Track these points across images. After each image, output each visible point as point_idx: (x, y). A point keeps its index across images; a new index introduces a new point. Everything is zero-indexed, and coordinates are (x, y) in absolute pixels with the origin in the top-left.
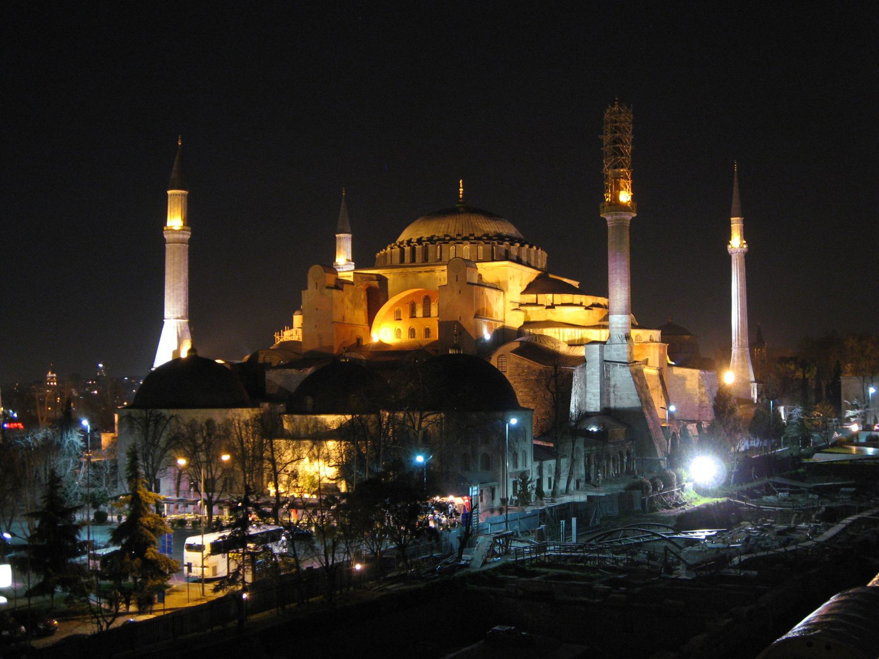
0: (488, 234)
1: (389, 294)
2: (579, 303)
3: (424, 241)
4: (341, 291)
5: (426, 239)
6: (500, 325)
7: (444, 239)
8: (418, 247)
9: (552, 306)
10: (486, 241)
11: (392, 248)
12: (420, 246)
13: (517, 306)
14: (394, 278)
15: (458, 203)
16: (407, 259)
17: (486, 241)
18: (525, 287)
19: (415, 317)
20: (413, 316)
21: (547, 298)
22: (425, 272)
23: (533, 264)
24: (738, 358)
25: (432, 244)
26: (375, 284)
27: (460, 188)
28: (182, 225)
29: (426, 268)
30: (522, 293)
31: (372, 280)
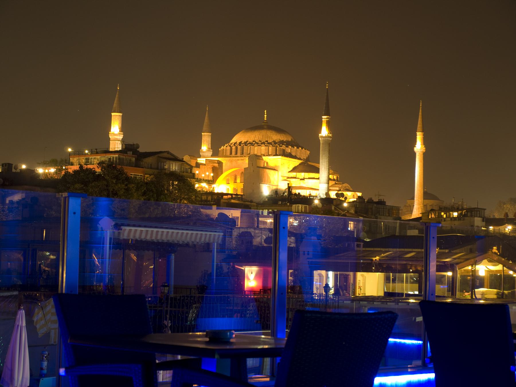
0: (275, 141)
1: (223, 170)
2: (318, 178)
3: (242, 144)
4: (198, 169)
5: (243, 143)
6: (274, 188)
7: (252, 143)
8: (239, 147)
9: (303, 179)
10: (273, 145)
11: (226, 147)
12: (240, 147)
13: (285, 178)
14: (226, 163)
15: (264, 123)
16: (233, 153)
17: (273, 145)
18: (292, 169)
19: (236, 182)
20: (235, 182)
21: (302, 175)
22: (241, 160)
23: (298, 157)
24: (417, 210)
25: (246, 145)
26: (216, 165)
27: (265, 115)
28: (119, 131)
29: (241, 158)
30: (289, 172)
31: (215, 163)
